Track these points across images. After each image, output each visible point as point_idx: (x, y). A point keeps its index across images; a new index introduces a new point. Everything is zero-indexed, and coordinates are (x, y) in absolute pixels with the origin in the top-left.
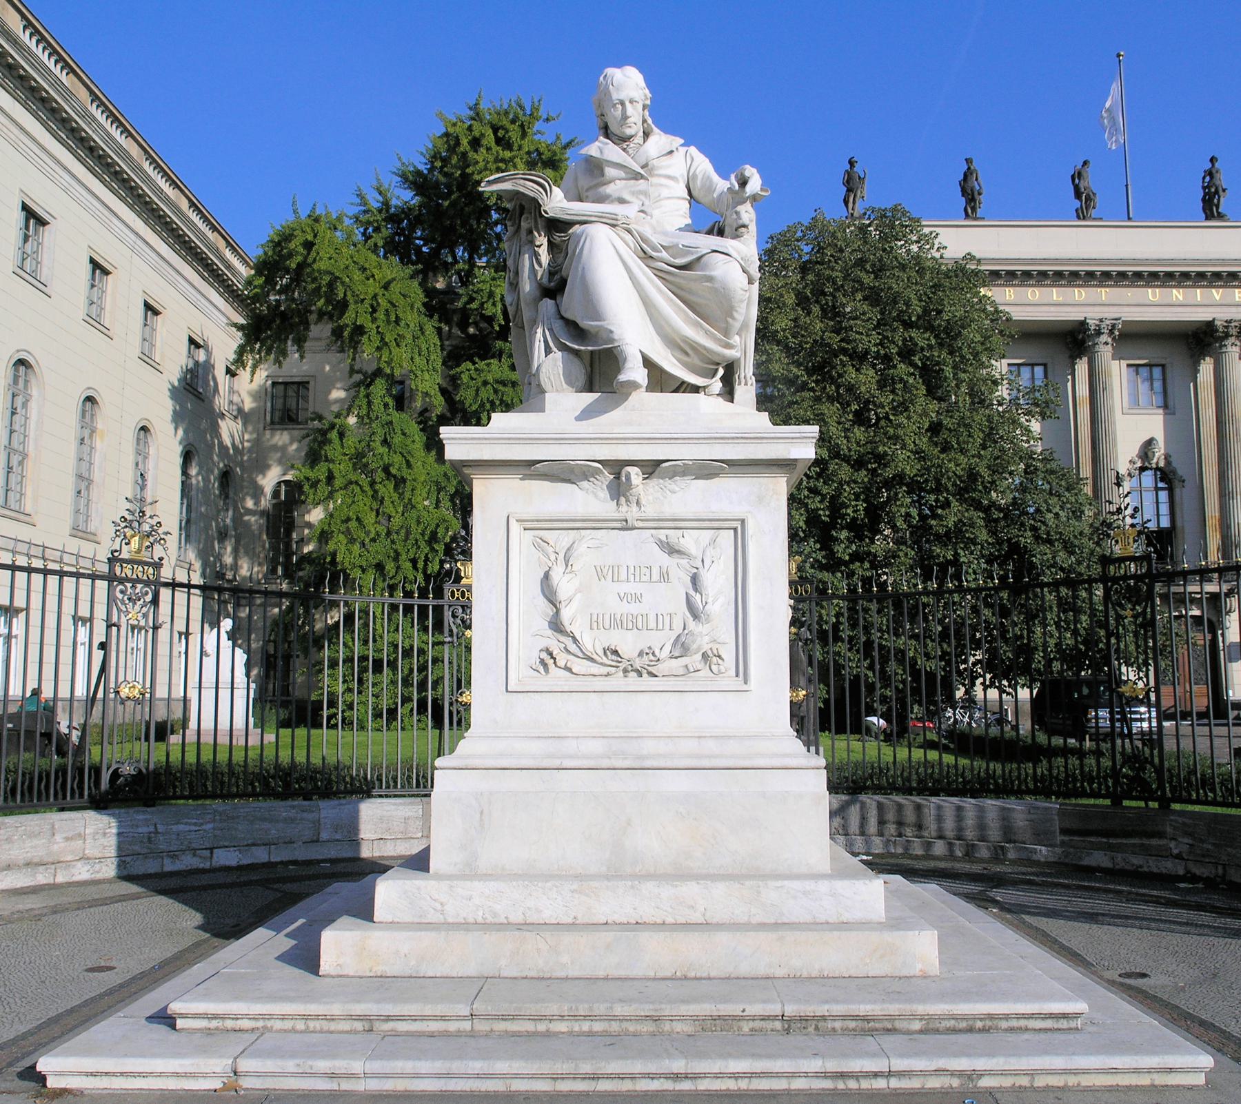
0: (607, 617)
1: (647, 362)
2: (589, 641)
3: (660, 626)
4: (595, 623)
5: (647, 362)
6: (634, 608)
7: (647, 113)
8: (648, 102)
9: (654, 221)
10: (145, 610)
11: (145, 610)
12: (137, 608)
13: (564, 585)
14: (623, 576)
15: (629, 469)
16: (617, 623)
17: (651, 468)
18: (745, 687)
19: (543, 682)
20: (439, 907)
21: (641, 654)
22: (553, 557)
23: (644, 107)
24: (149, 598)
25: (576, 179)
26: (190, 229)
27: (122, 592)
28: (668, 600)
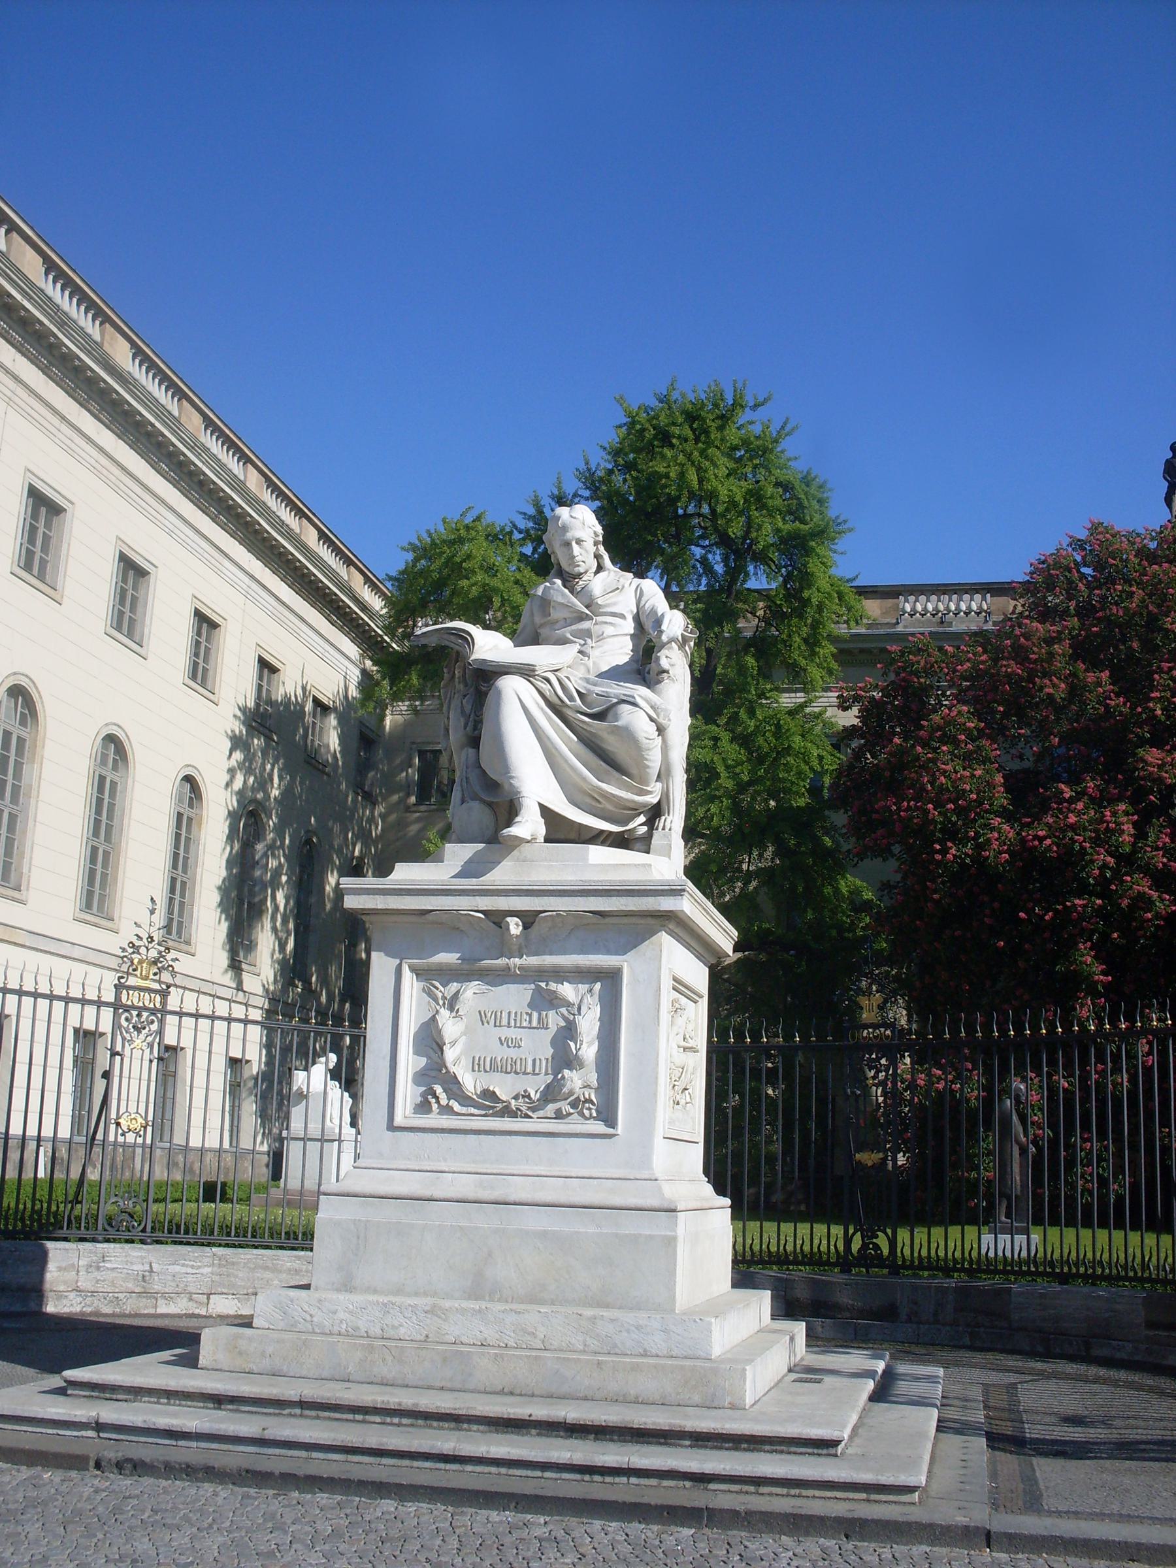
0: (488, 1060)
1: (545, 811)
2: (470, 1083)
3: (537, 1071)
4: (477, 1066)
5: (545, 811)
6: (513, 1053)
7: (601, 548)
8: (601, 539)
9: (590, 663)
10: (150, 1039)
11: (150, 1039)
12: (142, 1036)
13: (450, 1027)
14: (505, 1022)
15: (509, 919)
16: (496, 1067)
17: (529, 919)
18: (611, 1131)
19: (434, 1119)
20: (308, 1318)
21: (516, 1098)
22: (441, 1002)
23: (596, 543)
24: (155, 1027)
25: (532, 615)
26: (316, 566)
27: (127, 1019)
28: (537, 1047)
